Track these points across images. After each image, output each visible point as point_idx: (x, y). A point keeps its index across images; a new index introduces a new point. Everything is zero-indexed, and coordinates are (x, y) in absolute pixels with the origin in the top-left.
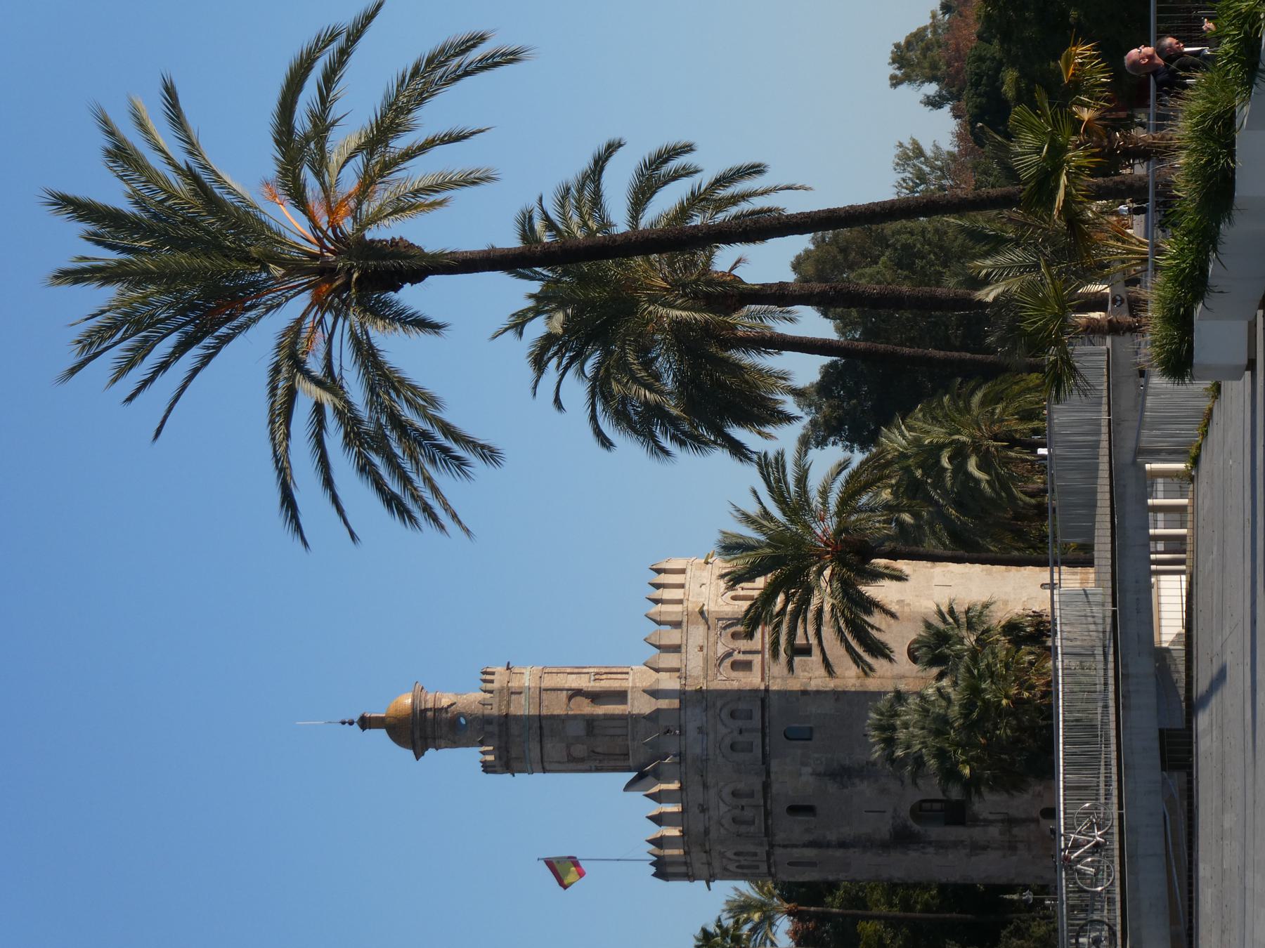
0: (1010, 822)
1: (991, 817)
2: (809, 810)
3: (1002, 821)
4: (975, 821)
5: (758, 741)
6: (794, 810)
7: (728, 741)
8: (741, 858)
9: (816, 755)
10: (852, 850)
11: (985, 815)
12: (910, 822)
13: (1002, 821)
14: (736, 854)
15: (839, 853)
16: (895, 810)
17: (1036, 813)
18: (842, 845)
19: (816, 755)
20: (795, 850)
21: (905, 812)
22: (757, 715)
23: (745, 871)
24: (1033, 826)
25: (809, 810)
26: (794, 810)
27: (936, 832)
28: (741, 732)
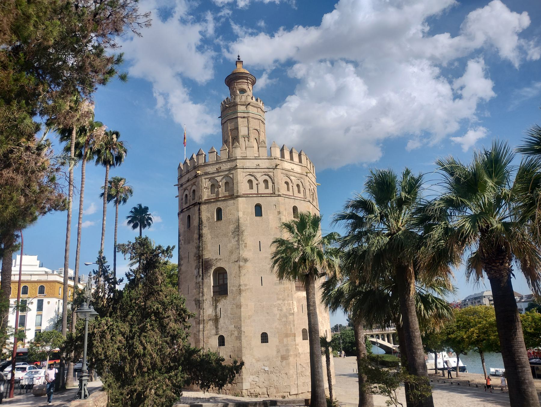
0: (216, 320)
1: (218, 309)
2: (219, 218)
3: (216, 316)
4: (216, 301)
5: (254, 191)
6: (219, 211)
7: (252, 178)
8: (191, 194)
9: (248, 219)
10: (197, 241)
11: (220, 305)
12: (214, 268)
13: (216, 316)
14: (194, 191)
15: (196, 236)
16: (220, 259)
17: (221, 333)
18: (200, 236)
19: (248, 219)
20: (197, 215)
21: (220, 265)
22: (267, 191)
23: (184, 199)
24: (214, 332)
25: (219, 218)
26: (219, 211)
27: (210, 281)
28: (257, 184)
